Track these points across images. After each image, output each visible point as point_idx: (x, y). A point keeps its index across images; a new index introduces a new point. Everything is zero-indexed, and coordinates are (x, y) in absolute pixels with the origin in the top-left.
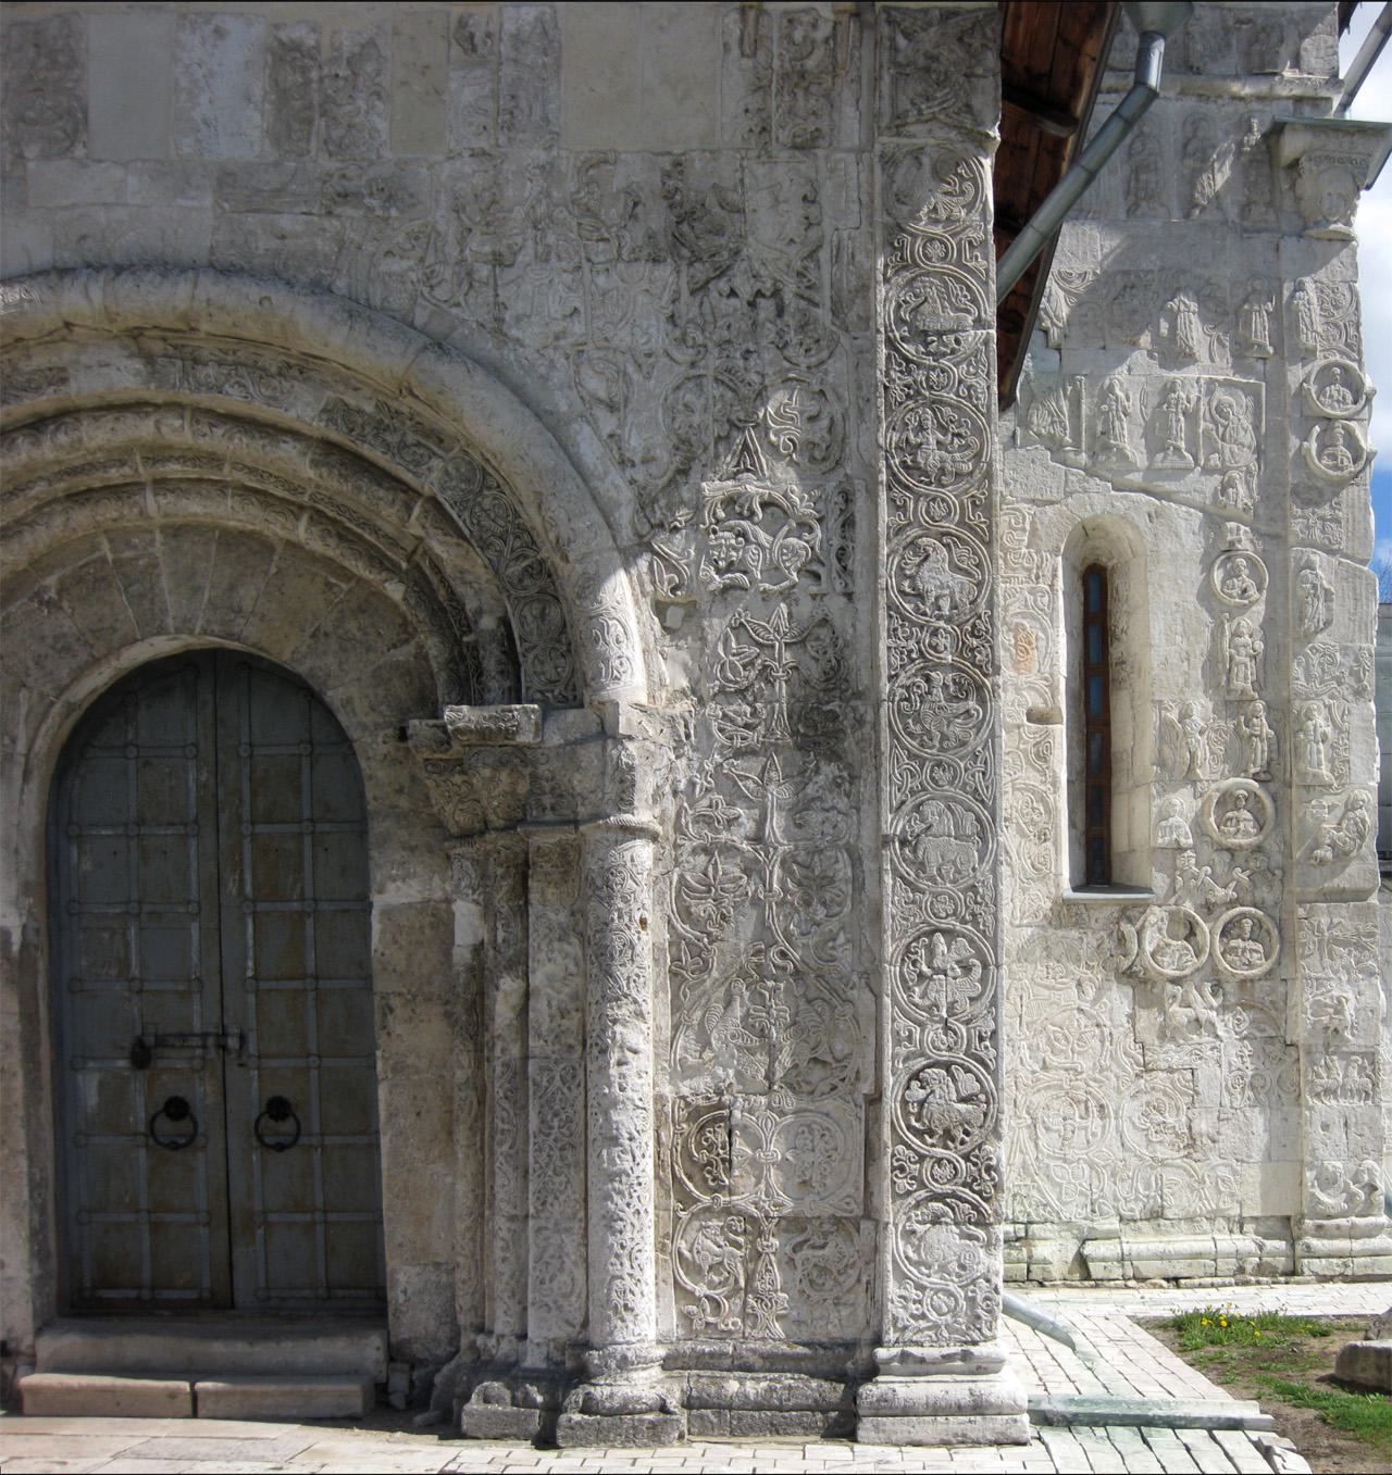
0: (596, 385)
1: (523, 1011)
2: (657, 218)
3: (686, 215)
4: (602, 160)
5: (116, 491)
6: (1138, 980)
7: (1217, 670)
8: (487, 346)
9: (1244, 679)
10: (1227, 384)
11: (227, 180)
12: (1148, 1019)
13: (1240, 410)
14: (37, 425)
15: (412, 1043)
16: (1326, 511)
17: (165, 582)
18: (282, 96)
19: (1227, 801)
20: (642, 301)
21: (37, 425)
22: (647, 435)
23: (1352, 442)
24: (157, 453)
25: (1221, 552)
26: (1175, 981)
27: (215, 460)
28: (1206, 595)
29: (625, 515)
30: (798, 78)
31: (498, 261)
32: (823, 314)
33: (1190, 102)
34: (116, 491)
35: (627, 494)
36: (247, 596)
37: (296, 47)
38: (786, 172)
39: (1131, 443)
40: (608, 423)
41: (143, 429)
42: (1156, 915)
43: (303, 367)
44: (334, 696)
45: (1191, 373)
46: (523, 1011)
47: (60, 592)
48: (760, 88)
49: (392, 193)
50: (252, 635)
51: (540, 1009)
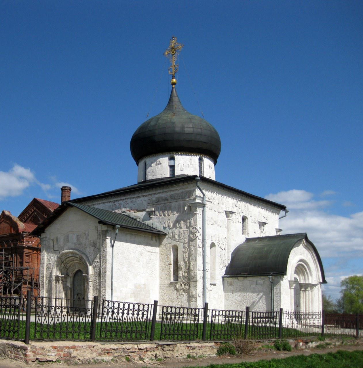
0: (90, 254)
3: (94, 244)
4: (91, 241)
5: (73, 261)
6: (176, 289)
7: (184, 259)
8: (85, 253)
9: (186, 259)
10: (185, 230)
11: (75, 243)
12: (178, 293)
13: (186, 232)
14: (68, 258)
16: (193, 242)
18: (77, 238)
19: (184, 272)
20: (92, 248)
21: (68, 258)
22: (92, 258)
23: (195, 235)
24: (74, 259)
25: (184, 247)
26: (180, 290)
28: (183, 252)
29: (91, 262)
31: (86, 247)
33: (183, 201)
34: (73, 261)
38: (99, 241)
39: (177, 237)
41: (72, 258)
42: (179, 283)
43: (78, 254)
45: (182, 229)
48: (98, 235)
49: (81, 244)
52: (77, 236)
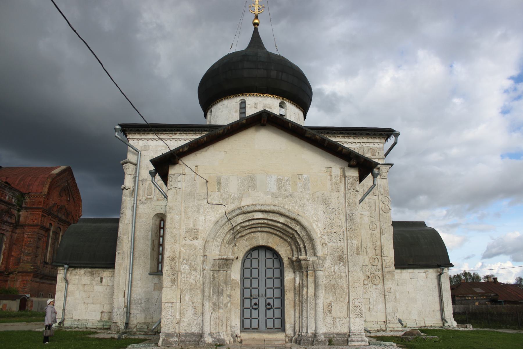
0: (315, 219)
1: (307, 292)
2: (321, 200)
11: (273, 194)
15: (289, 296)
17: (260, 239)
18: (279, 185)
27: (269, 225)
30: (336, 184)
32: (340, 211)
35: (319, 232)
36: (270, 241)
37: (280, 179)
40: (316, 223)
44: (280, 253)
46: (307, 292)
47: (247, 239)
50: (270, 245)
51: (309, 292)
52: (279, 180)
